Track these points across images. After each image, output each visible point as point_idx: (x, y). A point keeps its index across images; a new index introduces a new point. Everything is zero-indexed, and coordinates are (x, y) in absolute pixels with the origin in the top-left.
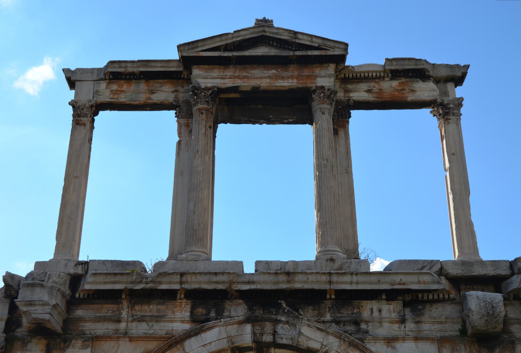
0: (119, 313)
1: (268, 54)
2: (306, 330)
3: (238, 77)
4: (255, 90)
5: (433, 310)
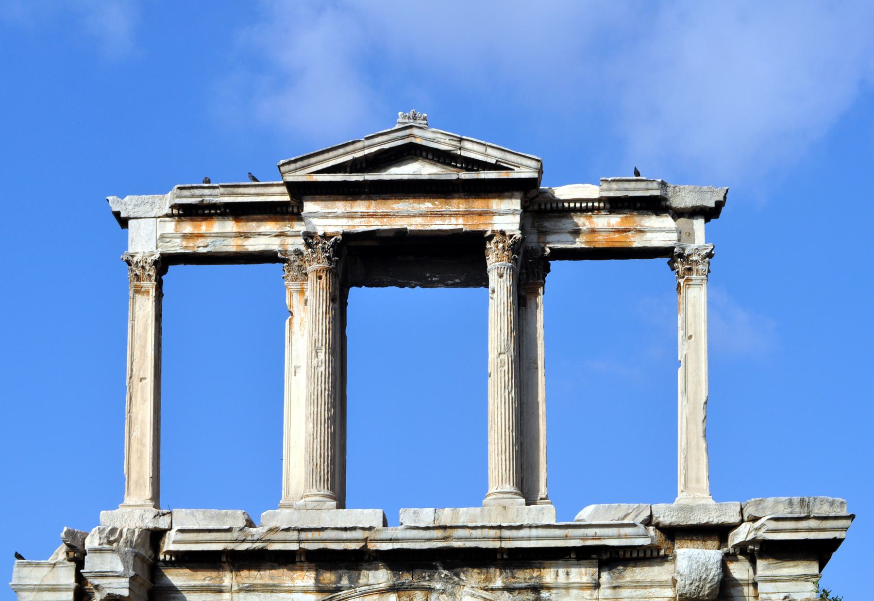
0: (220, 580)
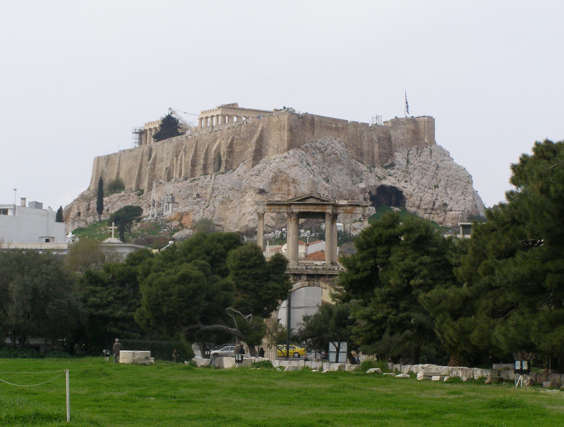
2: (321, 283)
3: (304, 209)
4: (310, 212)
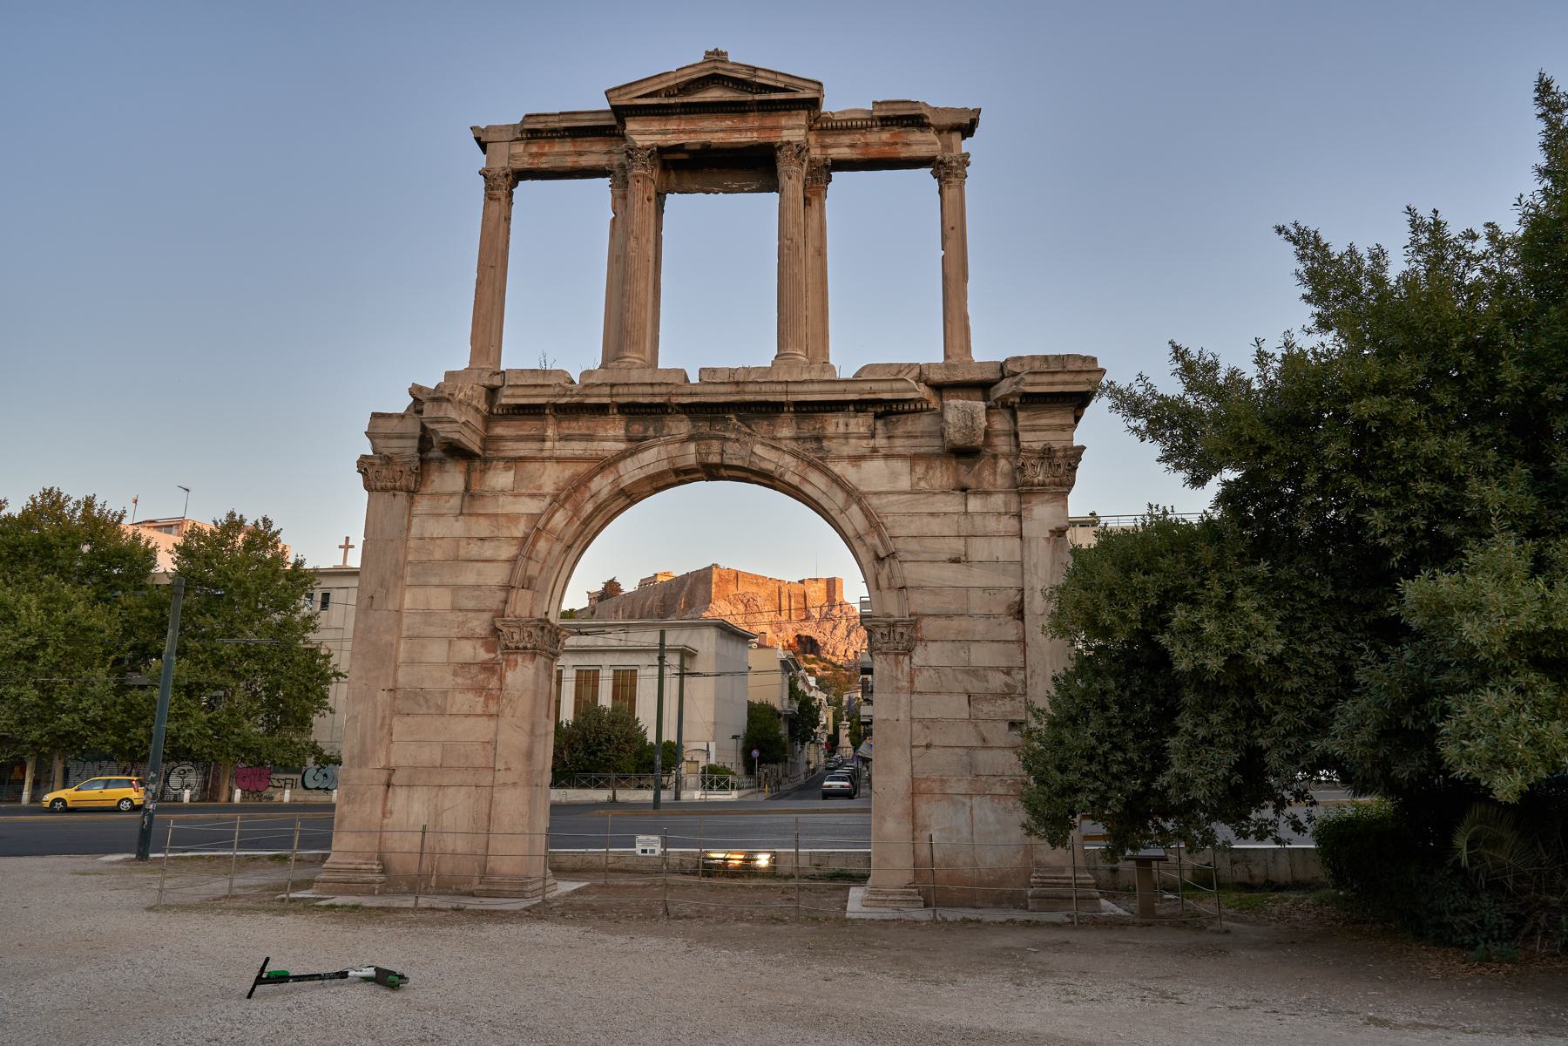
1: (720, 99)
2: (759, 449)
3: (683, 132)
4: (706, 149)
5: (909, 423)
